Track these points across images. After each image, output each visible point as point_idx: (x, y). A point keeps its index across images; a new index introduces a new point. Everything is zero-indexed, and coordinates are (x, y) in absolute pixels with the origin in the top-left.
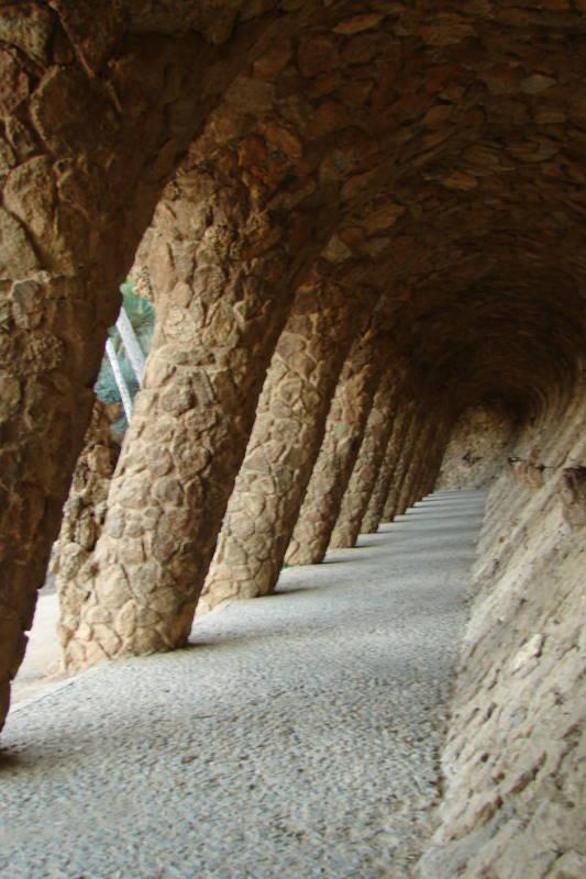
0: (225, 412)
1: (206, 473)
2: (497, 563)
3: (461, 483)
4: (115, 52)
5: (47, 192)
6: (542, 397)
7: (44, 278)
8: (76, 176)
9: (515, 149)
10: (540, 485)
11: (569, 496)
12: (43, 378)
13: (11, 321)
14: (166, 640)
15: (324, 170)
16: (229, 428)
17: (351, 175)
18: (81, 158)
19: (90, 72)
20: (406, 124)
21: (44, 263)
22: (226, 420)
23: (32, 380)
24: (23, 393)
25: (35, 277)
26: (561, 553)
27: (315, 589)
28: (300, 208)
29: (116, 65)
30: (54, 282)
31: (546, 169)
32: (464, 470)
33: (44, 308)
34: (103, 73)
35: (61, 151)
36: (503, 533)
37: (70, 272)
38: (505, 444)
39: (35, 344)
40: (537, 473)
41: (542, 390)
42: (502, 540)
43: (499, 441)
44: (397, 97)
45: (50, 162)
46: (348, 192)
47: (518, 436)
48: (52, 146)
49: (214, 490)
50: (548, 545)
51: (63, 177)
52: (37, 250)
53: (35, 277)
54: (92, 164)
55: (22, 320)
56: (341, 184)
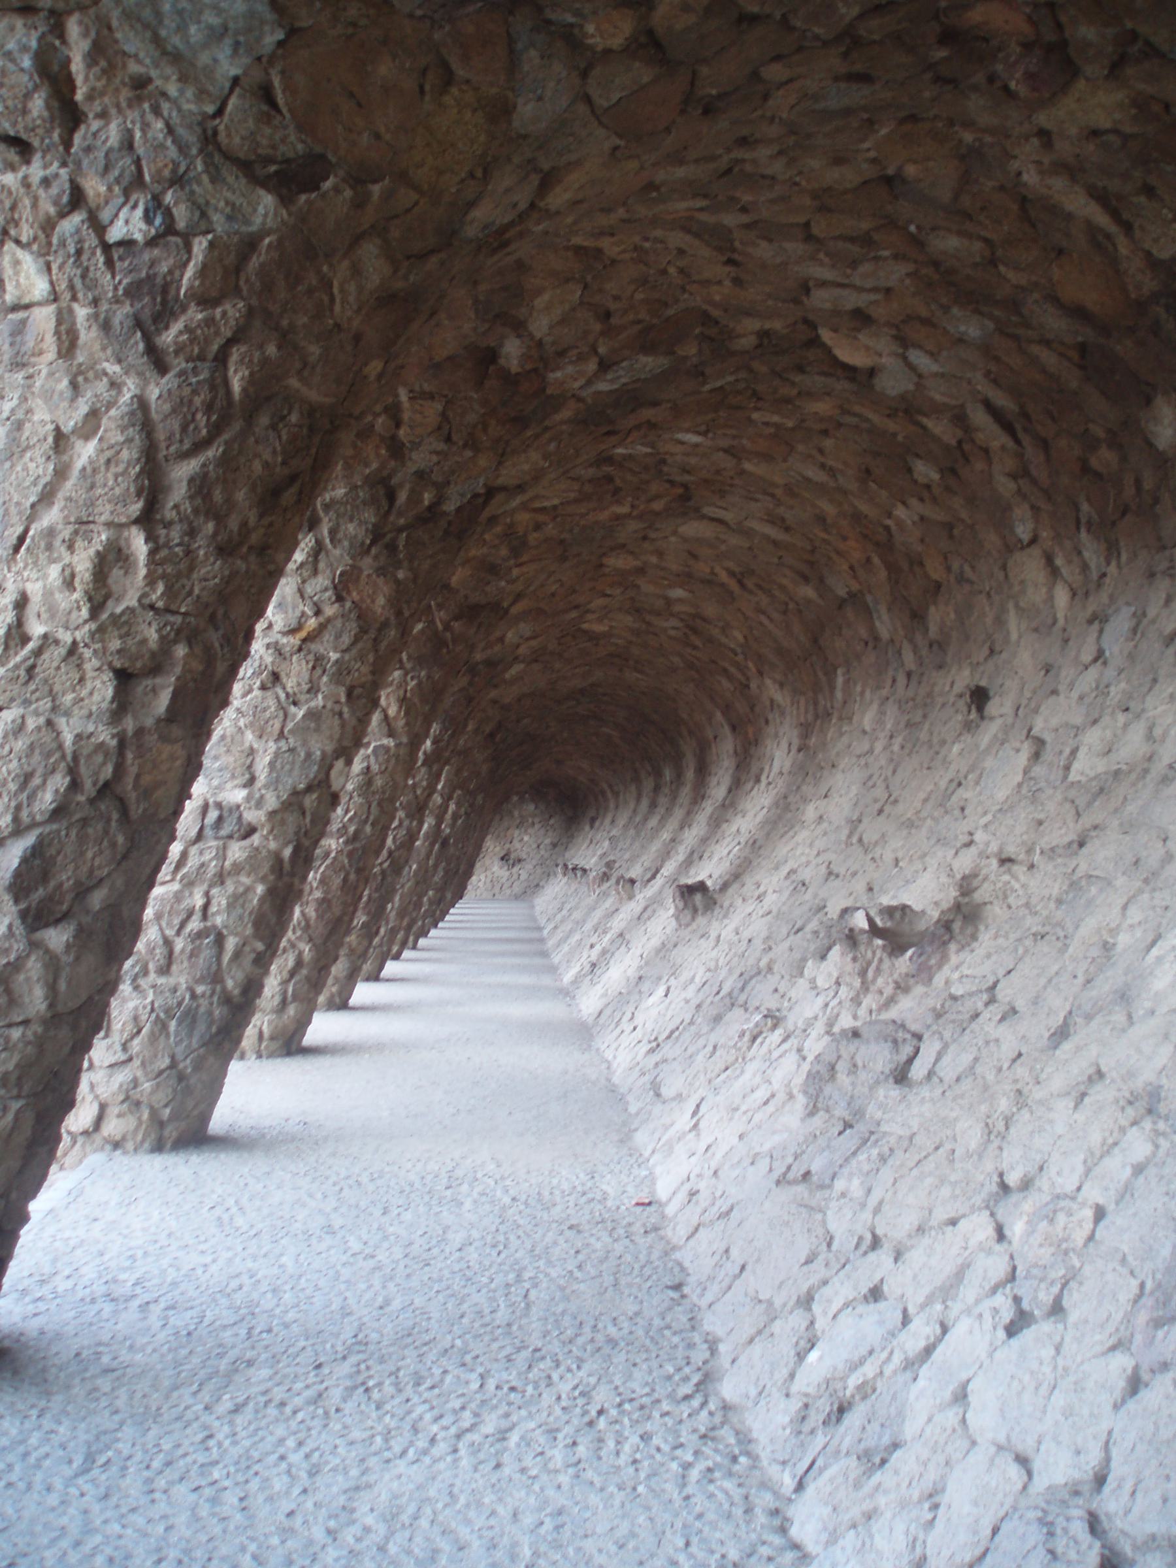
0: (407, 816)
1: (386, 865)
2: (594, 965)
3: (495, 892)
4: (456, 618)
5: (401, 692)
6: (609, 795)
7: (389, 742)
8: (419, 684)
9: (648, 618)
10: (631, 897)
11: (681, 905)
12: (379, 804)
13: (368, 768)
14: (337, 1000)
15: (510, 635)
16: (409, 829)
17: (528, 639)
18: (423, 673)
19: (440, 626)
20: (576, 607)
21: (391, 734)
22: (406, 823)
23: (374, 804)
24: (369, 813)
25: (385, 741)
26: (670, 946)
27: (402, 980)
28: (490, 663)
29: (456, 625)
30: (397, 746)
31: (672, 633)
32: (498, 870)
33: (388, 761)
34: (447, 627)
35: (413, 669)
36: (594, 940)
37: (405, 740)
38: (554, 845)
39: (379, 782)
40: (628, 885)
41: (610, 786)
42: (592, 946)
43: (548, 841)
44: (574, 591)
45: (406, 674)
46: (522, 650)
47: (572, 837)
48: (408, 666)
49: (389, 879)
50: (655, 942)
51: (412, 684)
52: (389, 725)
53: (385, 741)
54: (429, 677)
55: (375, 768)
56: (518, 646)
